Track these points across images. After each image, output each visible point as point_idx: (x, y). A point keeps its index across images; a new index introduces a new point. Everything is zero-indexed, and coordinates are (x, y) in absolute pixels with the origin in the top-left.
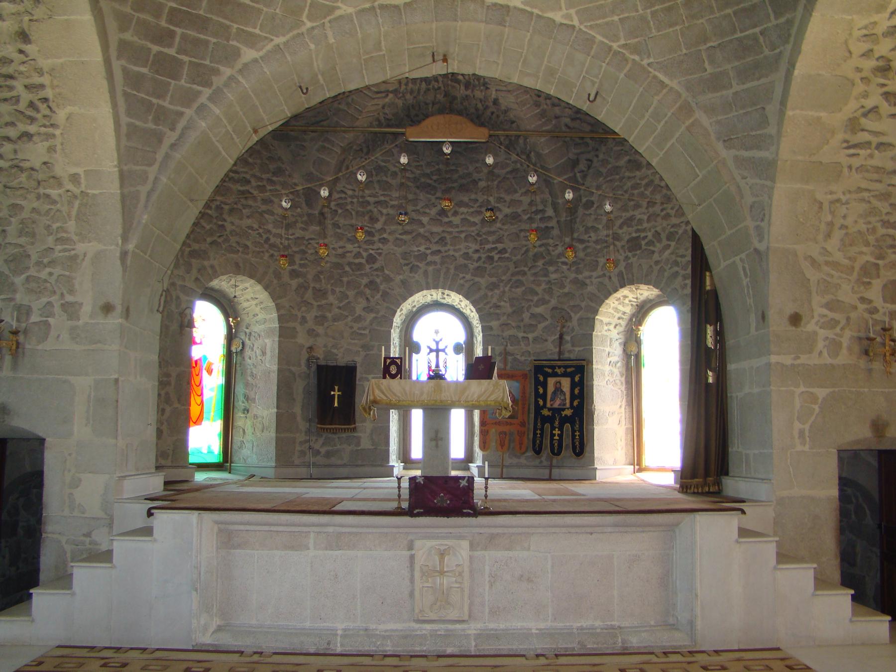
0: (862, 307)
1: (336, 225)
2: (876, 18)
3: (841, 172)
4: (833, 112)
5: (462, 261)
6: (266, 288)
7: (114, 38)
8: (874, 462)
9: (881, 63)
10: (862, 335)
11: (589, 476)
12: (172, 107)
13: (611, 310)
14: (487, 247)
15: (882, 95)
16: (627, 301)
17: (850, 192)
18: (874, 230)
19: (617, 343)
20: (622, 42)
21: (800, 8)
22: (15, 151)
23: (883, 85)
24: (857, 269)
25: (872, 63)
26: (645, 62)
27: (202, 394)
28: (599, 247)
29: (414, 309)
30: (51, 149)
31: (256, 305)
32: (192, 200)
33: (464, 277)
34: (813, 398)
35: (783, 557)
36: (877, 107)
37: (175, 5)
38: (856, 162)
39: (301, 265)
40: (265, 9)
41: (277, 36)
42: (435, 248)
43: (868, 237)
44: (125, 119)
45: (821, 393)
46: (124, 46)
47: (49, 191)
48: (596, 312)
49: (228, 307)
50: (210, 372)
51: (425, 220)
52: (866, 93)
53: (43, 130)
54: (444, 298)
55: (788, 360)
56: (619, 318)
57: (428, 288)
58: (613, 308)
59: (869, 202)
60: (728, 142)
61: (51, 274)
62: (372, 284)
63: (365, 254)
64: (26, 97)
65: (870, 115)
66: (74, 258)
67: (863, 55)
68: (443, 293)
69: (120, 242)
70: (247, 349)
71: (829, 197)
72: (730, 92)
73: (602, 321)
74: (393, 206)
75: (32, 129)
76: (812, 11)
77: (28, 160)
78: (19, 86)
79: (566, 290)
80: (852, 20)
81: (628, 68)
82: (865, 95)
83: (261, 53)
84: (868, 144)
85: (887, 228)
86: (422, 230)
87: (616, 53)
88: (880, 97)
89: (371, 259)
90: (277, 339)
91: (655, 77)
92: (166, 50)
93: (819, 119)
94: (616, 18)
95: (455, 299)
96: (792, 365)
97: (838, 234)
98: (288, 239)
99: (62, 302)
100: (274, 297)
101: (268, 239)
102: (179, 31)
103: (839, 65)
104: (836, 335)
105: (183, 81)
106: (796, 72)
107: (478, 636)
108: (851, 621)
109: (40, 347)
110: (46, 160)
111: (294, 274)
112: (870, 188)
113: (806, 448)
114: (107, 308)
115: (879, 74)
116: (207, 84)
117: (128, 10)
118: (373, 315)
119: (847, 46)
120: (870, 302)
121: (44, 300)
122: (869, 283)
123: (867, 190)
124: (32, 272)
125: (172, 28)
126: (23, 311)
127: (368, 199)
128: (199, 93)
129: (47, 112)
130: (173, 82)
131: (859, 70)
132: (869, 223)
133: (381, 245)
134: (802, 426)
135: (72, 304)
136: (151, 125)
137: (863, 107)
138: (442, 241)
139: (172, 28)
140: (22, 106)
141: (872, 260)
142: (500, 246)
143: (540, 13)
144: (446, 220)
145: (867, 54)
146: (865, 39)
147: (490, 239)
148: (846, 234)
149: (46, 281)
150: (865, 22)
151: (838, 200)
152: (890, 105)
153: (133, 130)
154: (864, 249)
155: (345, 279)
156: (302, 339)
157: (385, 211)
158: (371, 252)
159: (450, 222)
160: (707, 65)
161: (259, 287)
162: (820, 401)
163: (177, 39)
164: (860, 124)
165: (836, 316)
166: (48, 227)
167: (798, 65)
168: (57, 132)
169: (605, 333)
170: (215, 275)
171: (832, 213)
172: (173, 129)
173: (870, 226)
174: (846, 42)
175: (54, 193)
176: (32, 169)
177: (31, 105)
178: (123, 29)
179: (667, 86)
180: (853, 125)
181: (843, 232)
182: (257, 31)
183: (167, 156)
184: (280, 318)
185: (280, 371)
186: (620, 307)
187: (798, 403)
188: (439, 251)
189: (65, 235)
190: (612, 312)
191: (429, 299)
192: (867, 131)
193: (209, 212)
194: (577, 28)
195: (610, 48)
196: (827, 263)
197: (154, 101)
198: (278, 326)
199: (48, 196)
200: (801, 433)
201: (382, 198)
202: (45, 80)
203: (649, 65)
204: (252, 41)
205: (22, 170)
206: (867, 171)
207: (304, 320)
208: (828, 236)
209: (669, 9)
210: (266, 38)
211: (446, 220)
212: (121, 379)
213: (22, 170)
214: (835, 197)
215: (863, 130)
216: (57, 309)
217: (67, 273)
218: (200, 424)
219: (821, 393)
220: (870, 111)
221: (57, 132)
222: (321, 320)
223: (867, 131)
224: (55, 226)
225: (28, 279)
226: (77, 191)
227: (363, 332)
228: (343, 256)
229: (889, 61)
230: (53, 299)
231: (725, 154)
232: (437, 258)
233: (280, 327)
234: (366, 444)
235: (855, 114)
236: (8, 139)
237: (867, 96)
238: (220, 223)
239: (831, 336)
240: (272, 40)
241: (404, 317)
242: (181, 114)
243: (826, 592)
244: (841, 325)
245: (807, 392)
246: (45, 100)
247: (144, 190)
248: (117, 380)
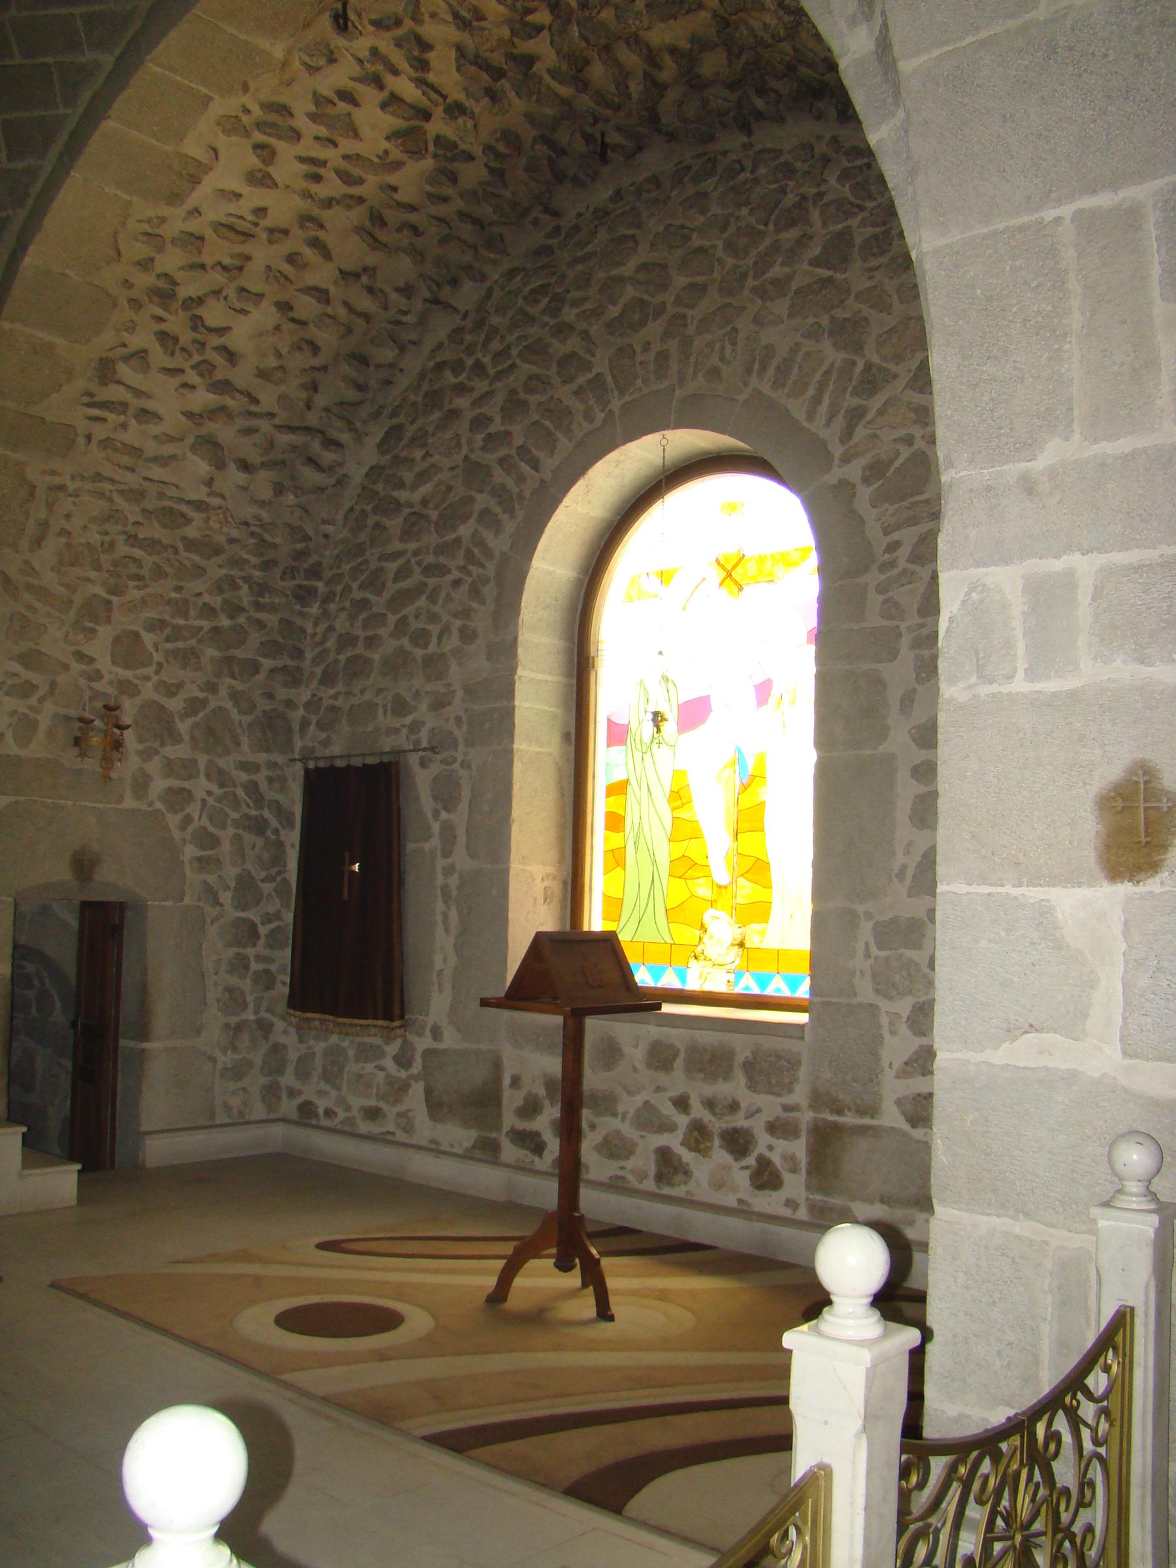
0: (76, 667)
2: (165, 211)
3: (74, 441)
4: (76, 341)
8: (73, 922)
9: (161, 284)
10: (74, 713)
15: (156, 334)
17: (83, 478)
18: (112, 544)
21: (53, 155)
23: (161, 320)
24: (76, 606)
25: (146, 280)
36: (145, 351)
38: (100, 432)
43: (101, 555)
52: (131, 324)
59: (111, 500)
65: (133, 362)
67: (139, 263)
71: (48, 479)
76: (72, 167)
80: (130, 203)
82: (132, 328)
84: (124, 406)
85: (132, 546)
88: (153, 337)
93: (52, 347)
97: (53, 544)
103: (98, 269)
104: (31, 708)
106: (27, 261)
108: (21, 1177)
112: (117, 478)
115: (156, 300)
119: (116, 241)
120: (92, 660)
123: (112, 481)
131: (128, 284)
132: (107, 533)
137: (124, 345)
141: (103, 594)
145: (146, 264)
146: (145, 238)
148: (69, 546)
150: (150, 213)
151: (62, 488)
152: (165, 353)
154: (93, 575)
164: (115, 372)
165: (34, 677)
167: (32, 249)
171: (50, 507)
173: (108, 539)
174: (116, 233)
180: (105, 370)
181: (64, 540)
192: (124, 384)
196: (29, 588)
206: (116, 450)
208: (38, 542)
214: (57, 480)
215: (119, 382)
220: (132, 355)
223: (124, 384)
229: (175, 284)
235: (111, 354)
237: (134, 329)
239: (22, 709)
244: (40, 693)
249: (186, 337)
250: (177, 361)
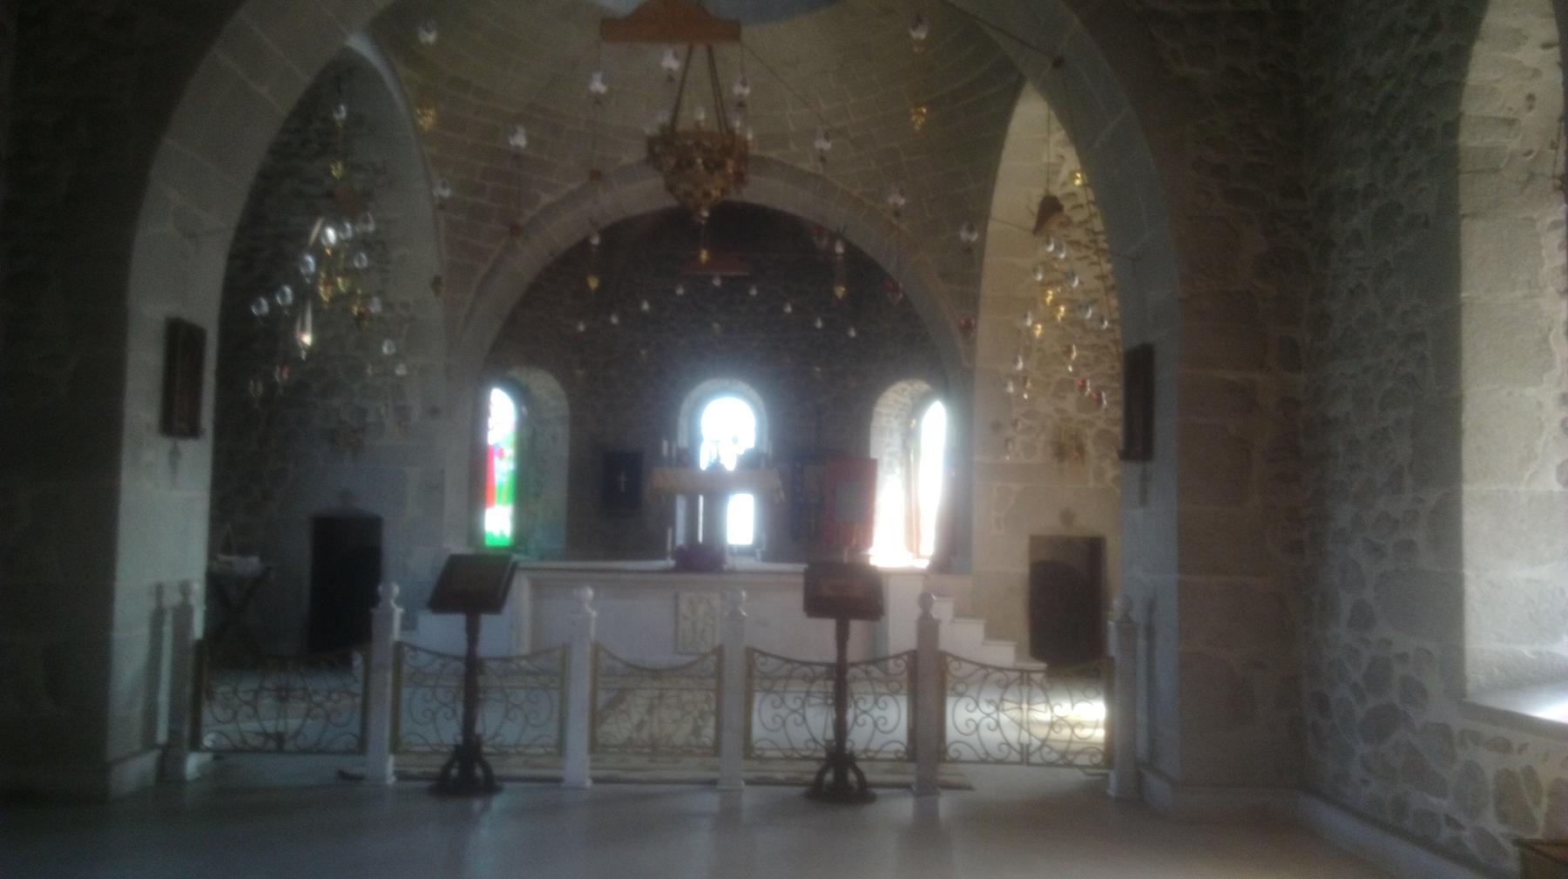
16: (906, 393)
49: (522, 395)
122: (1064, 397)
249: (1085, 239)
250: (1084, 252)
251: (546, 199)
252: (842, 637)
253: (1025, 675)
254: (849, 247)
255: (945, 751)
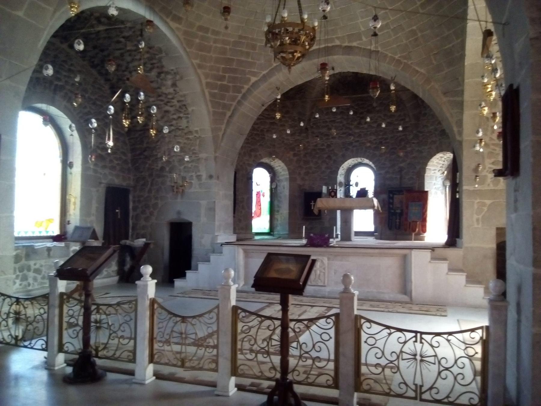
1: (313, 133)
5: (369, 145)
6: (283, 162)
7: (204, 81)
11: (422, 239)
12: (228, 103)
13: (435, 163)
14: (380, 137)
16: (443, 159)
19: (440, 179)
20: (399, 55)
22: (177, 123)
26: (410, 63)
27: (260, 205)
28: (428, 135)
29: (350, 166)
30: (188, 122)
31: (281, 169)
32: (241, 135)
33: (369, 152)
34: (484, 205)
35: (452, 269)
37: (224, 66)
39: (298, 151)
40: (258, 62)
41: (263, 71)
42: (357, 139)
44: (211, 110)
45: (488, 202)
46: (208, 84)
47: (189, 136)
48: (426, 164)
50: (264, 196)
51: (352, 127)
53: (185, 116)
54: (363, 161)
55: (471, 188)
56: (441, 167)
57: (353, 157)
58: (437, 163)
60: (445, 94)
61: (192, 165)
62: (329, 157)
63: (326, 144)
64: (178, 105)
66: (199, 159)
68: (361, 159)
69: (214, 153)
70: (278, 186)
72: (444, 72)
73: (430, 169)
74: (338, 122)
75: (181, 115)
77: (181, 126)
78: (175, 101)
79: (414, 155)
81: (402, 66)
83: (259, 78)
86: (350, 132)
87: (398, 60)
89: (329, 146)
90: (288, 182)
91: (414, 69)
92: (223, 83)
94: (395, 46)
95: (366, 161)
96: (474, 190)
98: (292, 140)
99: (196, 175)
100: (286, 165)
101: (283, 142)
102: (227, 75)
105: (231, 93)
107: (329, 292)
109: (190, 191)
110: (186, 125)
111: (295, 155)
113: (480, 226)
114: (211, 177)
116: (239, 92)
117: (207, 71)
118: (329, 170)
121: (190, 174)
124: (186, 165)
125: (224, 74)
126: (184, 178)
127: (326, 120)
128: (237, 96)
129: (185, 109)
130: (227, 94)
133: (332, 140)
134: (478, 217)
135: (199, 176)
136: (221, 110)
138: (360, 136)
139: (224, 74)
140: (177, 108)
142: (385, 136)
143: (365, 47)
144: (362, 126)
147: (381, 133)
149: (190, 168)
153: (215, 113)
155: (317, 156)
156: (299, 182)
157: (334, 125)
158: (329, 143)
159: (363, 127)
160: (434, 62)
161: (280, 162)
162: (488, 206)
163: (227, 77)
166: (190, 149)
168: (189, 116)
169: (433, 174)
170: (262, 158)
172: (229, 110)
175: (190, 137)
176: (183, 129)
177: (180, 107)
178: (206, 78)
179: (419, 72)
182: (256, 70)
183: (228, 122)
184: (290, 174)
185: (290, 195)
186: (441, 162)
187: (476, 206)
188: (358, 141)
189: (195, 152)
190: (436, 164)
191: (356, 162)
193: (258, 133)
194: (380, 51)
195: (394, 59)
197: (221, 101)
198: (288, 177)
199: (188, 139)
200: (478, 220)
201: (333, 119)
202: (182, 99)
203: (411, 63)
204: (254, 74)
205: (180, 130)
207: (300, 173)
209: (416, 40)
210: (259, 72)
211: (362, 126)
212: (216, 201)
213: (180, 130)
216: (194, 177)
217: (197, 165)
218: (260, 217)
219: (488, 202)
221: (189, 116)
222: (307, 173)
224: (193, 148)
225: (185, 167)
226: (197, 136)
227: (325, 178)
228: (316, 146)
230: (193, 174)
231: (445, 99)
232: (357, 144)
233: (290, 177)
234: (327, 224)
236: (174, 119)
238: (263, 137)
240: (262, 73)
241: (346, 170)
242: (231, 105)
243: (470, 285)
245: (481, 202)
246: (185, 105)
247: (221, 134)
248: (215, 202)
251: (254, 79)
252: (284, 304)
253: (419, 335)
254: (397, 85)
255: (361, 384)
